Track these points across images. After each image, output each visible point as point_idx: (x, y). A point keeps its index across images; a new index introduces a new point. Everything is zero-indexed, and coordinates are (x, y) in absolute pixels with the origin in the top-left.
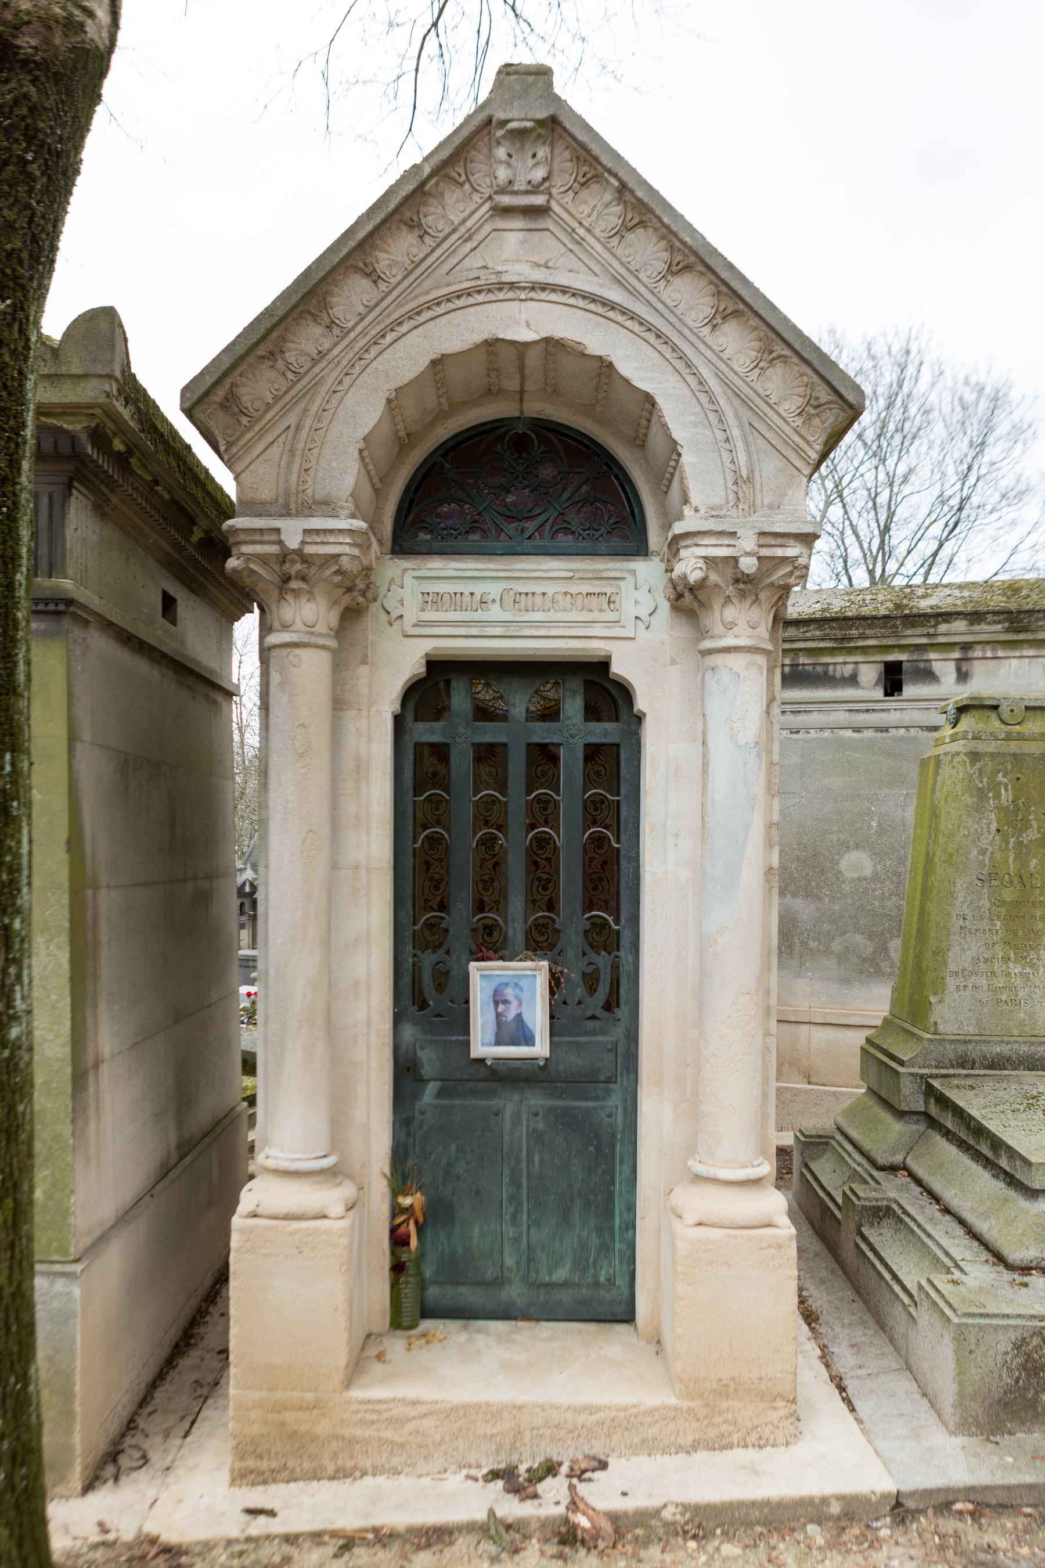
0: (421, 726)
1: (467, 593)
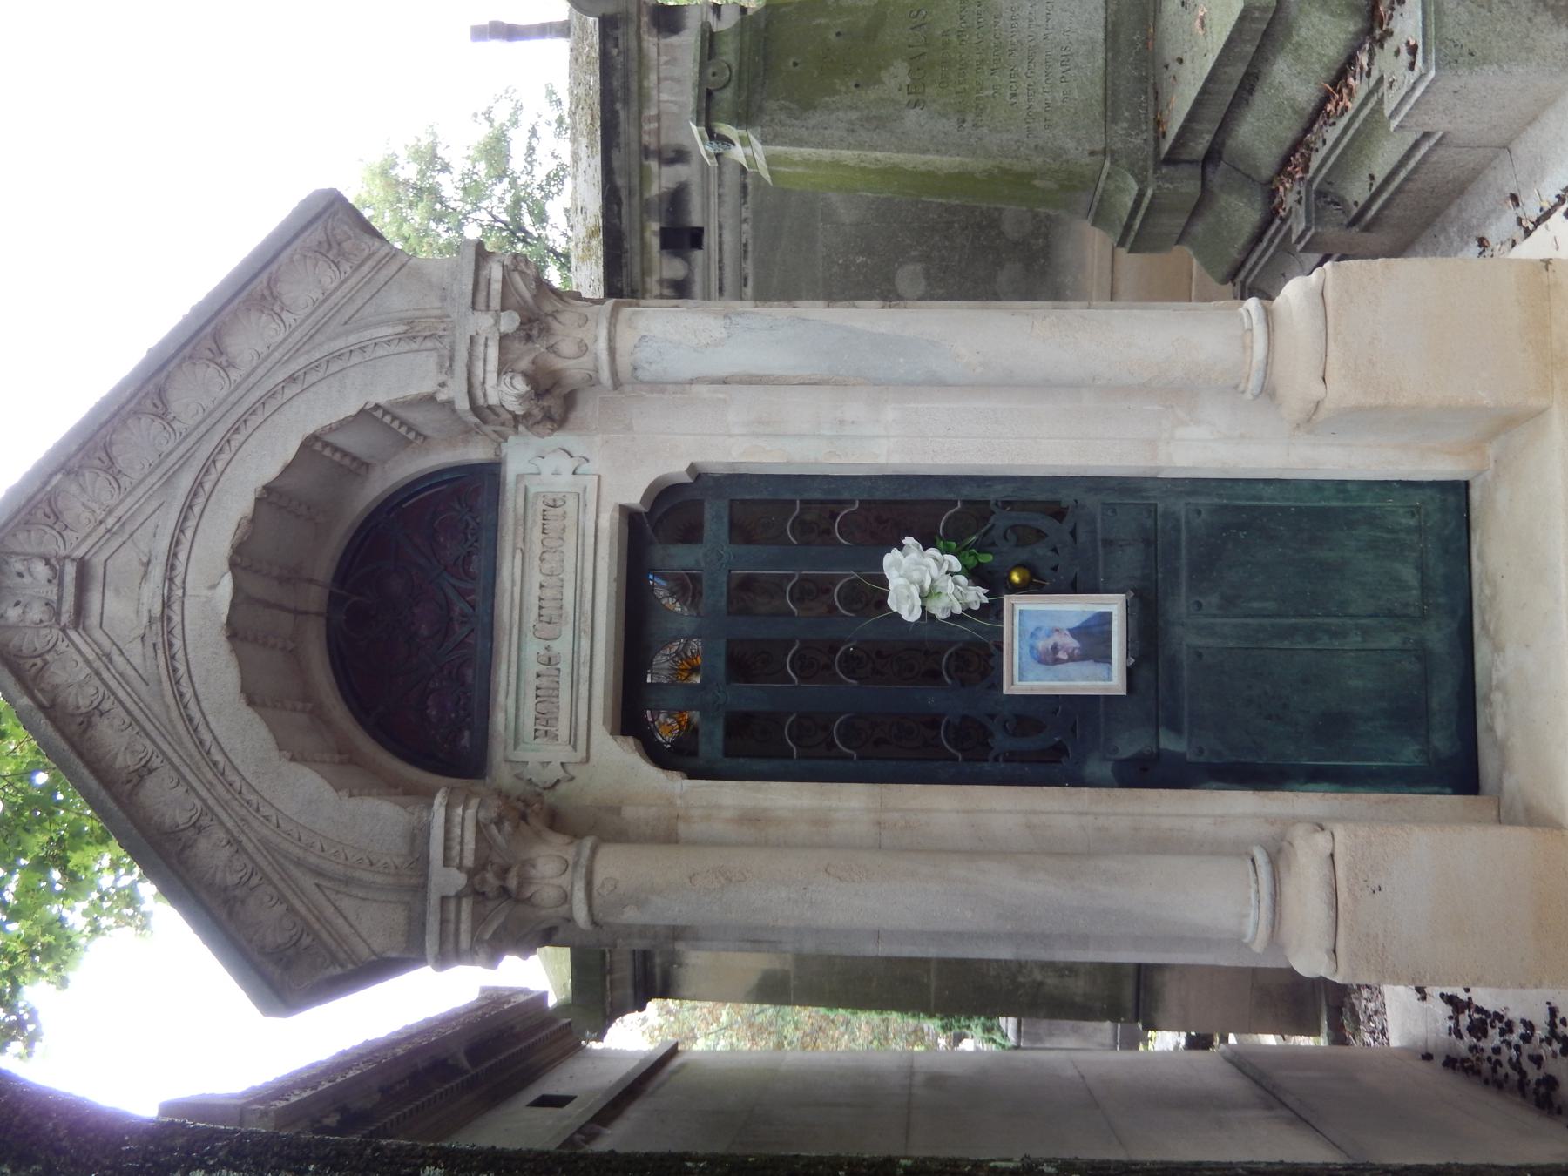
1: (537, 682)
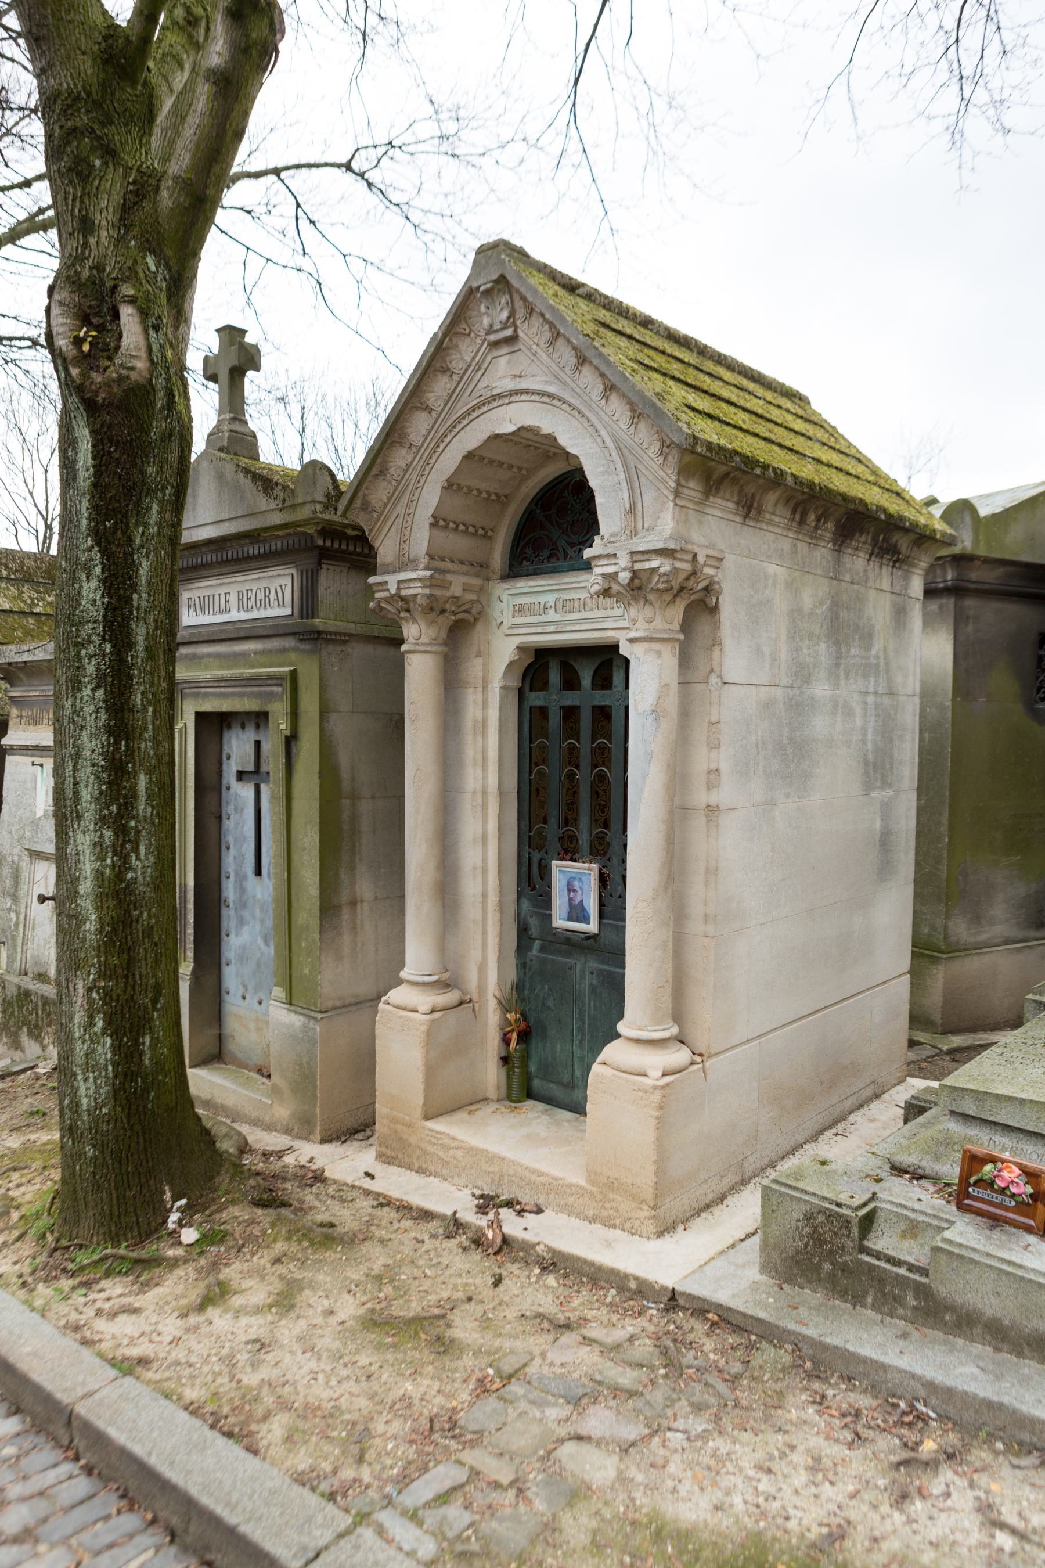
0: (533, 694)
